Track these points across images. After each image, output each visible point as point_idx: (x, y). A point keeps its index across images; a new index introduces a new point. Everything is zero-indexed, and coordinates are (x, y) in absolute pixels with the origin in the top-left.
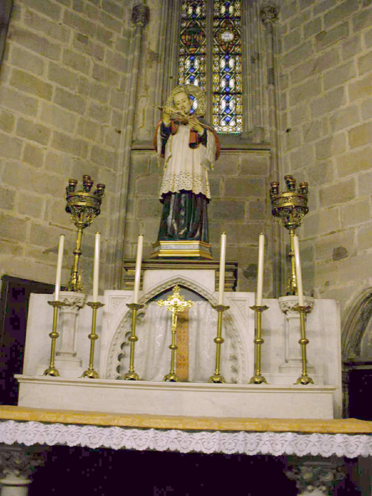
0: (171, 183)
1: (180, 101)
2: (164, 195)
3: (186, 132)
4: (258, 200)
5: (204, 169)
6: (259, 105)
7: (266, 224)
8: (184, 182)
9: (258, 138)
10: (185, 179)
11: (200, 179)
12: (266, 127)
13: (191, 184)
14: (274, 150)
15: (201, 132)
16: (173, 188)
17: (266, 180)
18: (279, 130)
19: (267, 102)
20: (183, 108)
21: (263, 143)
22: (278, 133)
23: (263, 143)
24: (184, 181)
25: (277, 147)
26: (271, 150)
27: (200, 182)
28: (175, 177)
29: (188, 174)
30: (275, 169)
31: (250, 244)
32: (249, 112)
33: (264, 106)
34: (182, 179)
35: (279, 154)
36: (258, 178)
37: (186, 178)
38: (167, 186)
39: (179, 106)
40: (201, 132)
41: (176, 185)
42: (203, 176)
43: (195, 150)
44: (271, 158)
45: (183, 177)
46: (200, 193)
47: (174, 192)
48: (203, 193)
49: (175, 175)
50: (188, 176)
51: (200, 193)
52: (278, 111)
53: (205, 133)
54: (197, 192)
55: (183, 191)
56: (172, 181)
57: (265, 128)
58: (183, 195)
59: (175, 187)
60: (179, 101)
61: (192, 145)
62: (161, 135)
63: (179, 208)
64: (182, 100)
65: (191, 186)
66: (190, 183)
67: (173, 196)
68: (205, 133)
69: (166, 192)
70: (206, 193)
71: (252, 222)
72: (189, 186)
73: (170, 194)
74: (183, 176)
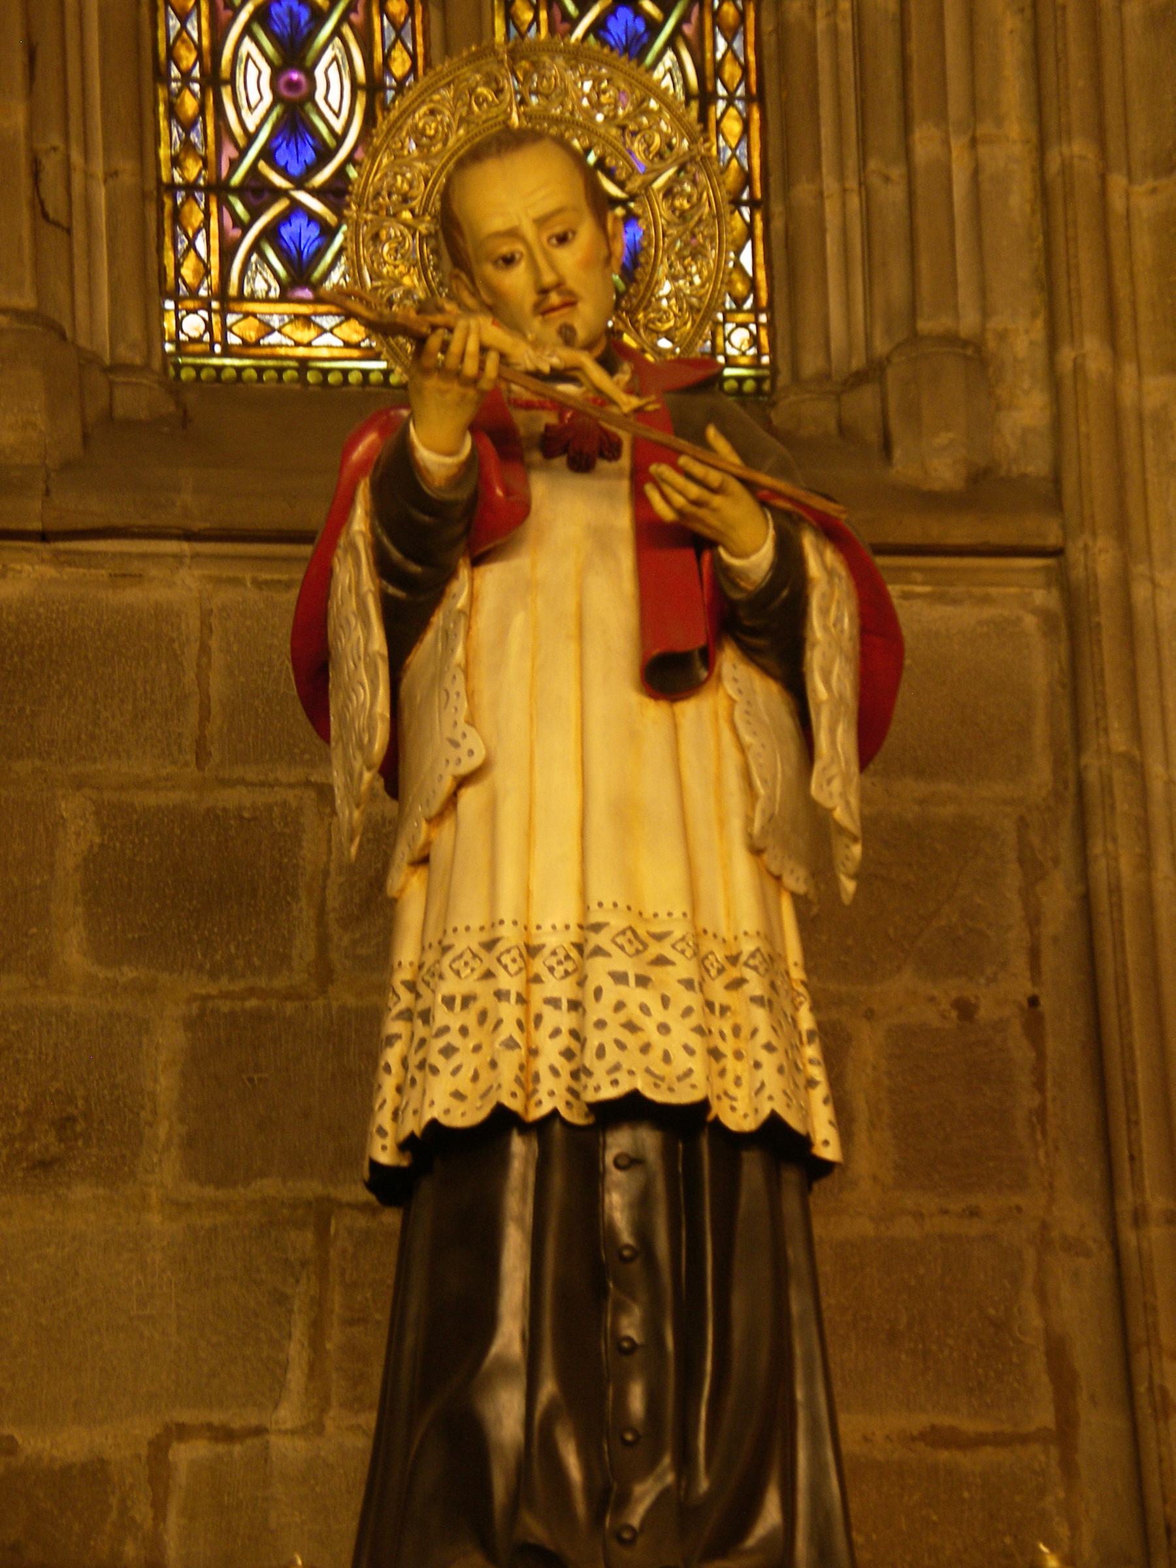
0: (509, 1029)
1: (529, 231)
2: (433, 1144)
3: (600, 537)
4: (965, 1009)
5: (770, 885)
6: (942, 117)
7: (1043, 1240)
8: (631, 1027)
9: (943, 439)
10: (634, 995)
11: (755, 985)
12: (1002, 336)
13: (695, 1041)
14: (1099, 558)
15: (754, 556)
16: (528, 1081)
17: (1022, 824)
18: (1129, 370)
19: (1013, 92)
20: (552, 298)
21: (984, 486)
22: (1128, 396)
23: (984, 486)
24: (633, 1011)
25: (1122, 530)
26: (1075, 553)
27: (760, 1016)
28: (538, 966)
29: (655, 949)
30: (1119, 740)
31: (920, 1421)
32: (830, 183)
33: (985, 128)
34: (613, 992)
35: (1141, 592)
36: (948, 811)
37: (643, 981)
38: (468, 1061)
39: (517, 282)
40: (754, 556)
41: (551, 1052)
42: (772, 960)
43: (688, 709)
44: (1072, 621)
45: (619, 978)
46: (774, 1122)
47: (536, 1114)
48: (793, 1120)
49: (532, 951)
50: (661, 961)
51: (774, 1122)
52: (1118, 181)
53: (788, 559)
54: (740, 1117)
55: (631, 1108)
56: (509, 1012)
57: (992, 344)
58: (619, 1142)
59: (541, 1065)
60: (513, 234)
61: (668, 675)
62: (384, 567)
63: (582, 1269)
64: (541, 222)
65: (697, 1064)
66: (682, 1032)
67: (518, 1146)
68: (788, 559)
69: (465, 1116)
70: (806, 1113)
71: (918, 1216)
72: (681, 1061)
73: (502, 1120)
74: (621, 962)
